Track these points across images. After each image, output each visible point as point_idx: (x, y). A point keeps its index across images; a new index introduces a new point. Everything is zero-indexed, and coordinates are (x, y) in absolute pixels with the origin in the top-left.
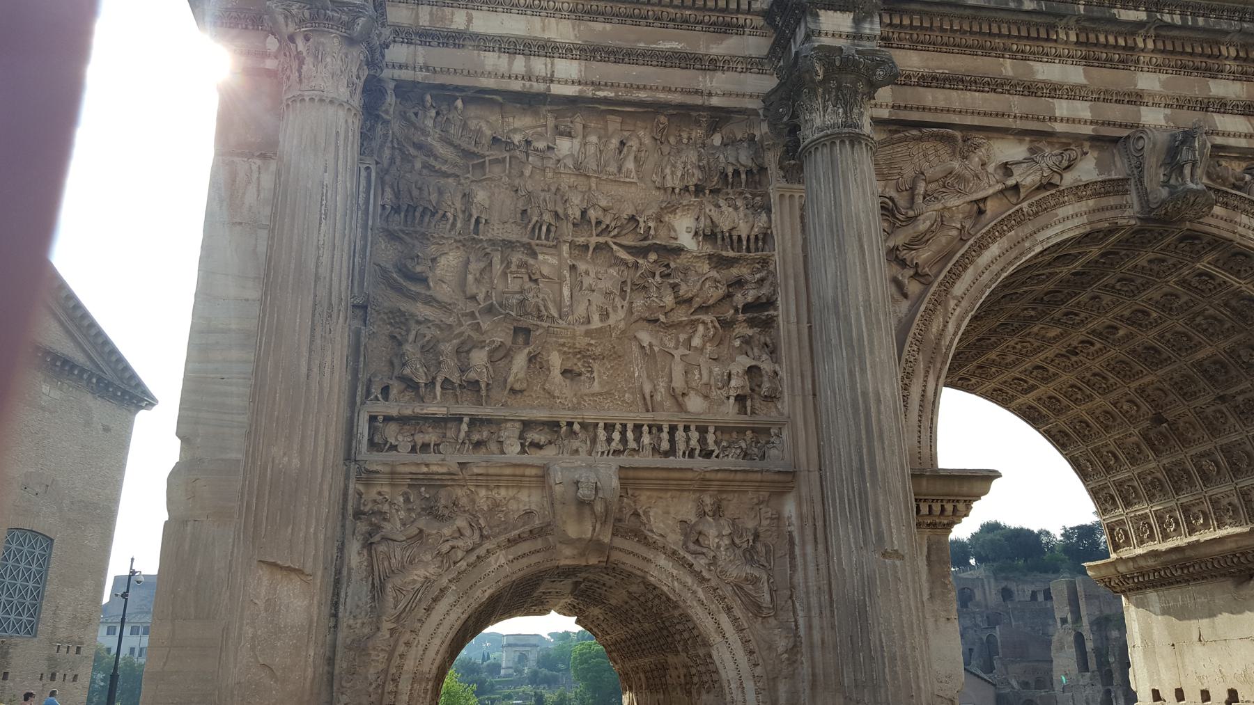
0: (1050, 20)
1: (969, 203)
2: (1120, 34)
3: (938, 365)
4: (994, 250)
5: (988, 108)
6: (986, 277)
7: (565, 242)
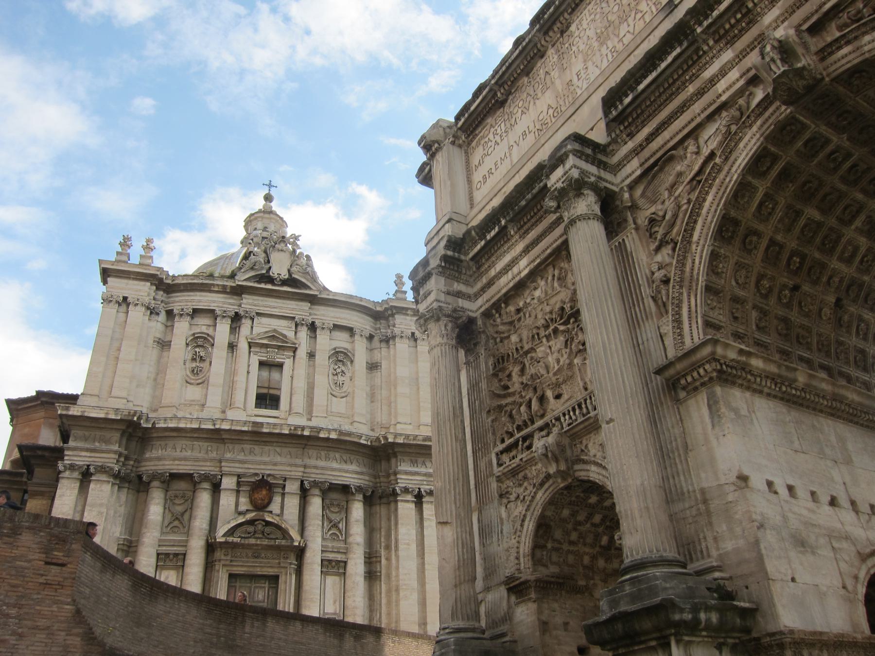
0: (693, 48)
1: (689, 183)
2: (736, 12)
3: (694, 288)
4: (710, 198)
5: (683, 124)
6: (709, 218)
7: (543, 337)
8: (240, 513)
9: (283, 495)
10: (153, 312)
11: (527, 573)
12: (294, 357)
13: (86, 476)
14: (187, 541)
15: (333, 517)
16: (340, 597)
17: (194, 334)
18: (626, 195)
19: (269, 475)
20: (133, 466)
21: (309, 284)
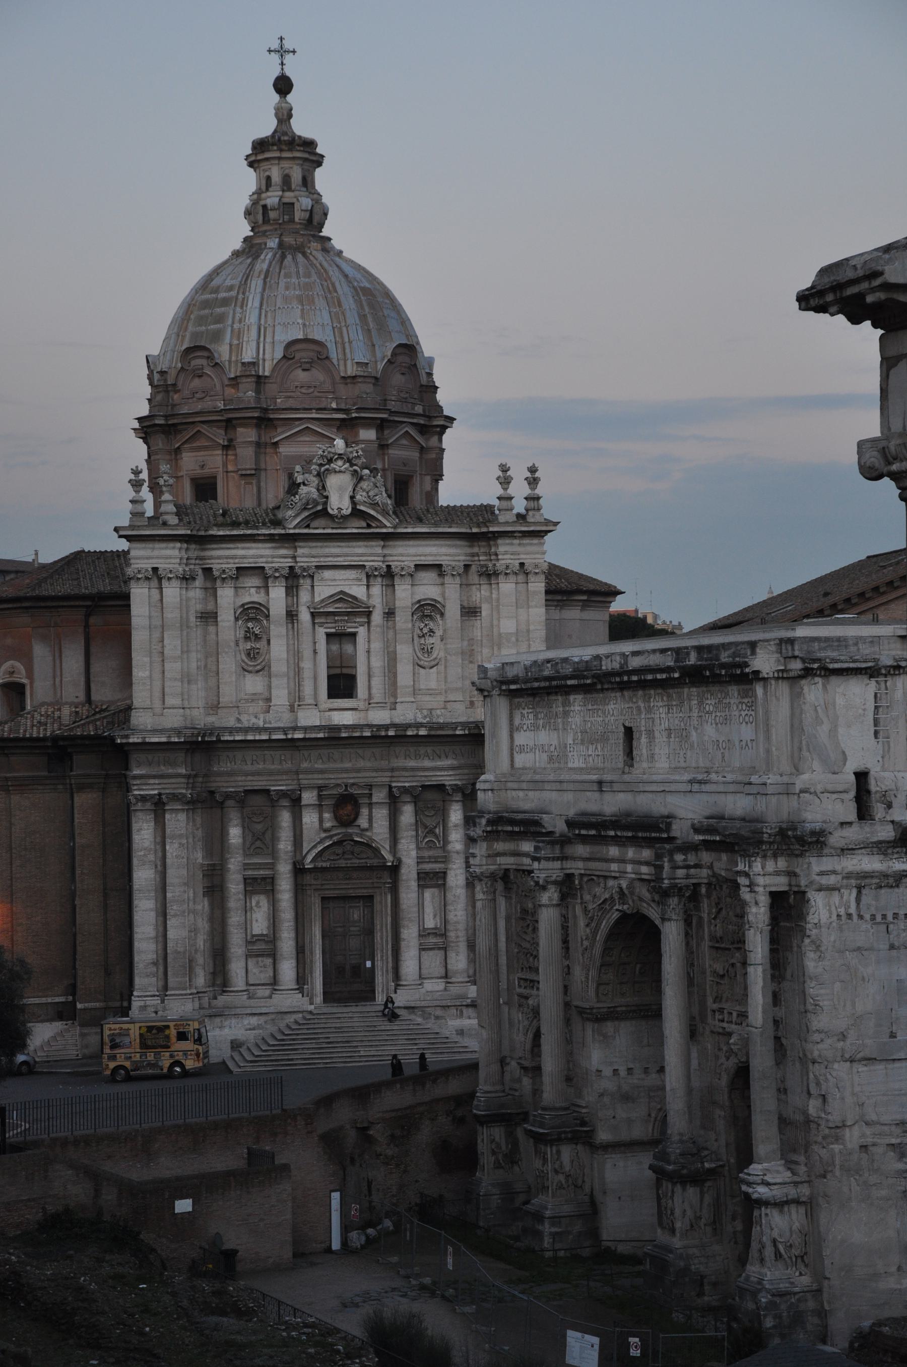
8: (325, 831)
9: (370, 805)
10: (187, 579)
11: (526, 1063)
12: (369, 623)
13: (159, 806)
14: (273, 864)
15: (430, 822)
16: (440, 909)
17: (243, 605)
18: (577, 882)
19: (353, 784)
20: (202, 783)
21: (380, 518)
